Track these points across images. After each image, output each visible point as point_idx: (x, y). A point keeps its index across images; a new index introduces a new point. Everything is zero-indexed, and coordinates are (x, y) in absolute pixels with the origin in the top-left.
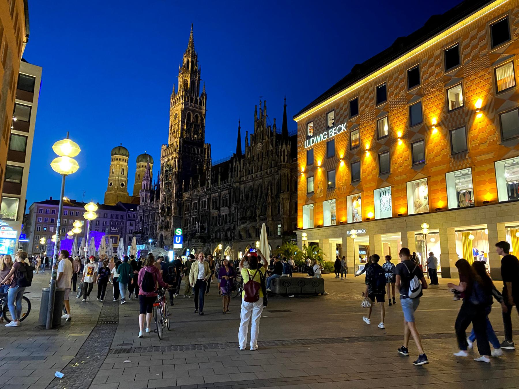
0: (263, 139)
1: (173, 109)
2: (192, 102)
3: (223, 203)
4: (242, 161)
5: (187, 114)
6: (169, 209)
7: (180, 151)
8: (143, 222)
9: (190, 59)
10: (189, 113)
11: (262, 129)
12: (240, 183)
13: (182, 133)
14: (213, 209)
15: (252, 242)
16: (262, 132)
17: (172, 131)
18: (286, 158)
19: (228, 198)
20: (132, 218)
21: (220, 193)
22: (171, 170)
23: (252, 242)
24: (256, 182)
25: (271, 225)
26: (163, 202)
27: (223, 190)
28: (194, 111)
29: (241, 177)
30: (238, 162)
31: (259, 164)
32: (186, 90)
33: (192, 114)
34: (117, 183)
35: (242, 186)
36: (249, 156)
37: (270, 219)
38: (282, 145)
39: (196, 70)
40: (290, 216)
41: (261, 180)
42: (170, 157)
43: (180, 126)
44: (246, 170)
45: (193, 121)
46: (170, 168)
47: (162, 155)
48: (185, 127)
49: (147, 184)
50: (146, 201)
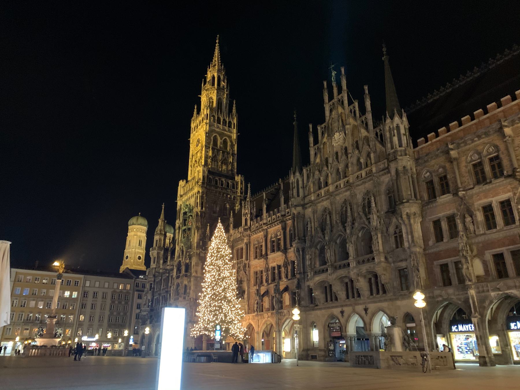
0: (343, 126)
1: (194, 135)
2: (219, 122)
3: (273, 246)
4: (304, 171)
5: (212, 138)
6: (188, 267)
7: (203, 183)
8: (153, 292)
9: (216, 75)
10: (216, 136)
11: (340, 110)
12: (304, 206)
13: (206, 161)
14: (256, 257)
15: (340, 309)
16: (340, 116)
17: (193, 162)
18: (404, 140)
19: (281, 237)
20: (140, 288)
21: (267, 232)
22: (191, 210)
23: (340, 309)
24: (338, 198)
25: (385, 269)
26: (179, 257)
27: (271, 224)
28: (221, 135)
29: (305, 197)
30: (298, 174)
31: (341, 167)
32: (212, 109)
33: (219, 138)
34: (133, 255)
35: (309, 211)
36: (318, 160)
37: (383, 259)
38: (392, 118)
39: (223, 86)
40: (424, 250)
41: (348, 193)
42: (190, 194)
43: (203, 152)
44: (314, 183)
45: (220, 147)
46: (189, 208)
47: (179, 195)
48: (210, 154)
49: (160, 240)
50: (158, 262)
